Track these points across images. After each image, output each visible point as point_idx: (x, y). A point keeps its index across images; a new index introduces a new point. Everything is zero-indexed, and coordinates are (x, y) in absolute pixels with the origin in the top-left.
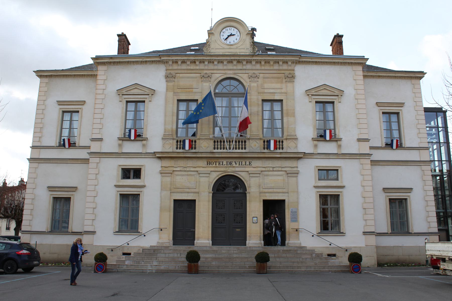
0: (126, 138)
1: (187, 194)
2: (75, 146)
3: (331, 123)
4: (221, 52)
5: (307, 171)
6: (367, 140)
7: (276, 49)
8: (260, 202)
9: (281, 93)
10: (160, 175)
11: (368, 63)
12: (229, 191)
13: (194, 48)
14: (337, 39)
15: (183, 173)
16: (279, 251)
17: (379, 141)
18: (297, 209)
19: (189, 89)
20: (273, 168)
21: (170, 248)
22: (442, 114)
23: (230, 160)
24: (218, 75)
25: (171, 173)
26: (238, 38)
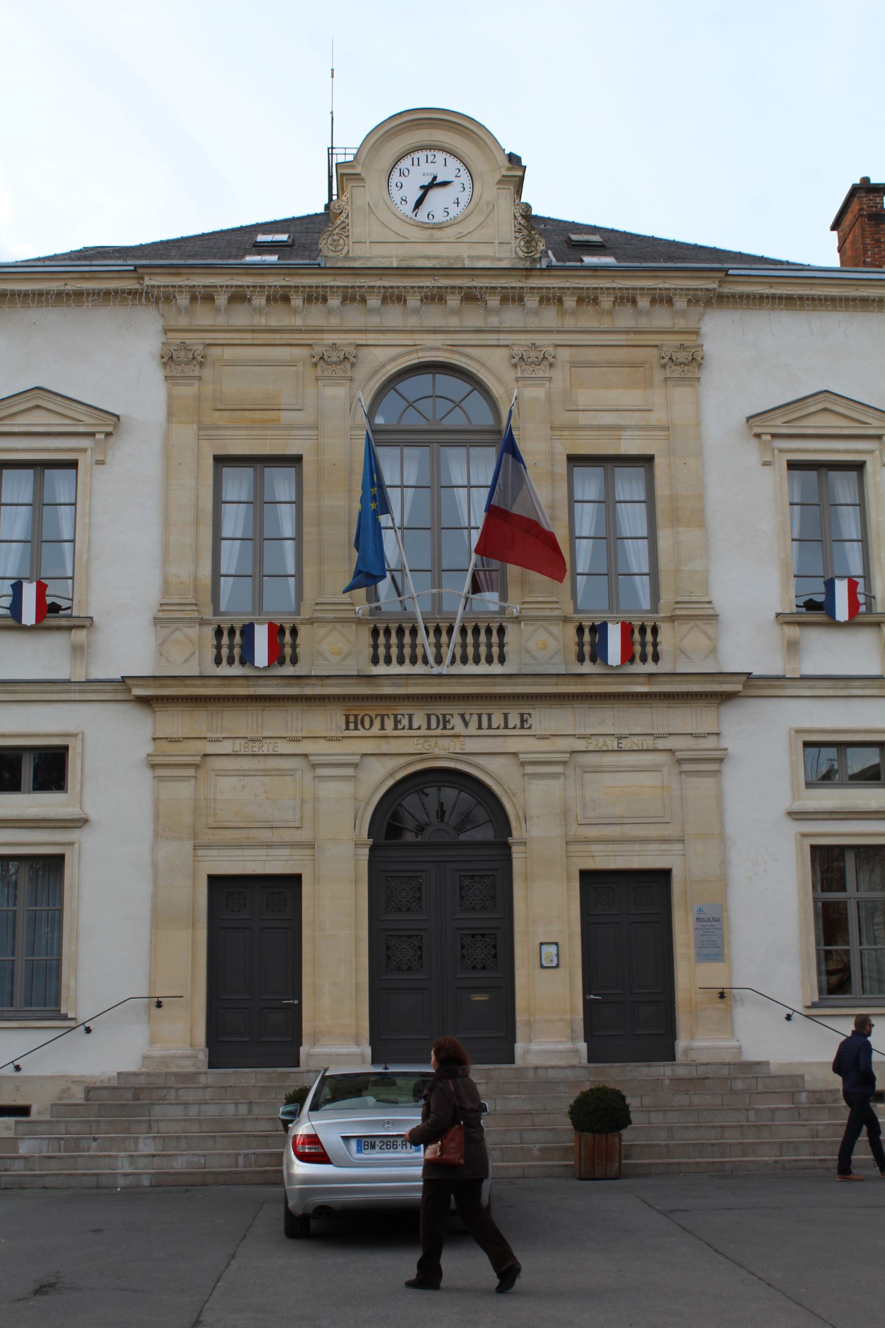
1: (263, 852)
3: (854, 552)
4: (392, 256)
5: (761, 750)
7: (610, 241)
8: (569, 879)
10: (148, 773)
14: (864, 199)
16: (658, 1082)
18: (722, 907)
19: (263, 411)
20: (620, 737)
21: (203, 1080)
23: (441, 709)
24: (381, 354)
25: (197, 766)
26: (464, 198)
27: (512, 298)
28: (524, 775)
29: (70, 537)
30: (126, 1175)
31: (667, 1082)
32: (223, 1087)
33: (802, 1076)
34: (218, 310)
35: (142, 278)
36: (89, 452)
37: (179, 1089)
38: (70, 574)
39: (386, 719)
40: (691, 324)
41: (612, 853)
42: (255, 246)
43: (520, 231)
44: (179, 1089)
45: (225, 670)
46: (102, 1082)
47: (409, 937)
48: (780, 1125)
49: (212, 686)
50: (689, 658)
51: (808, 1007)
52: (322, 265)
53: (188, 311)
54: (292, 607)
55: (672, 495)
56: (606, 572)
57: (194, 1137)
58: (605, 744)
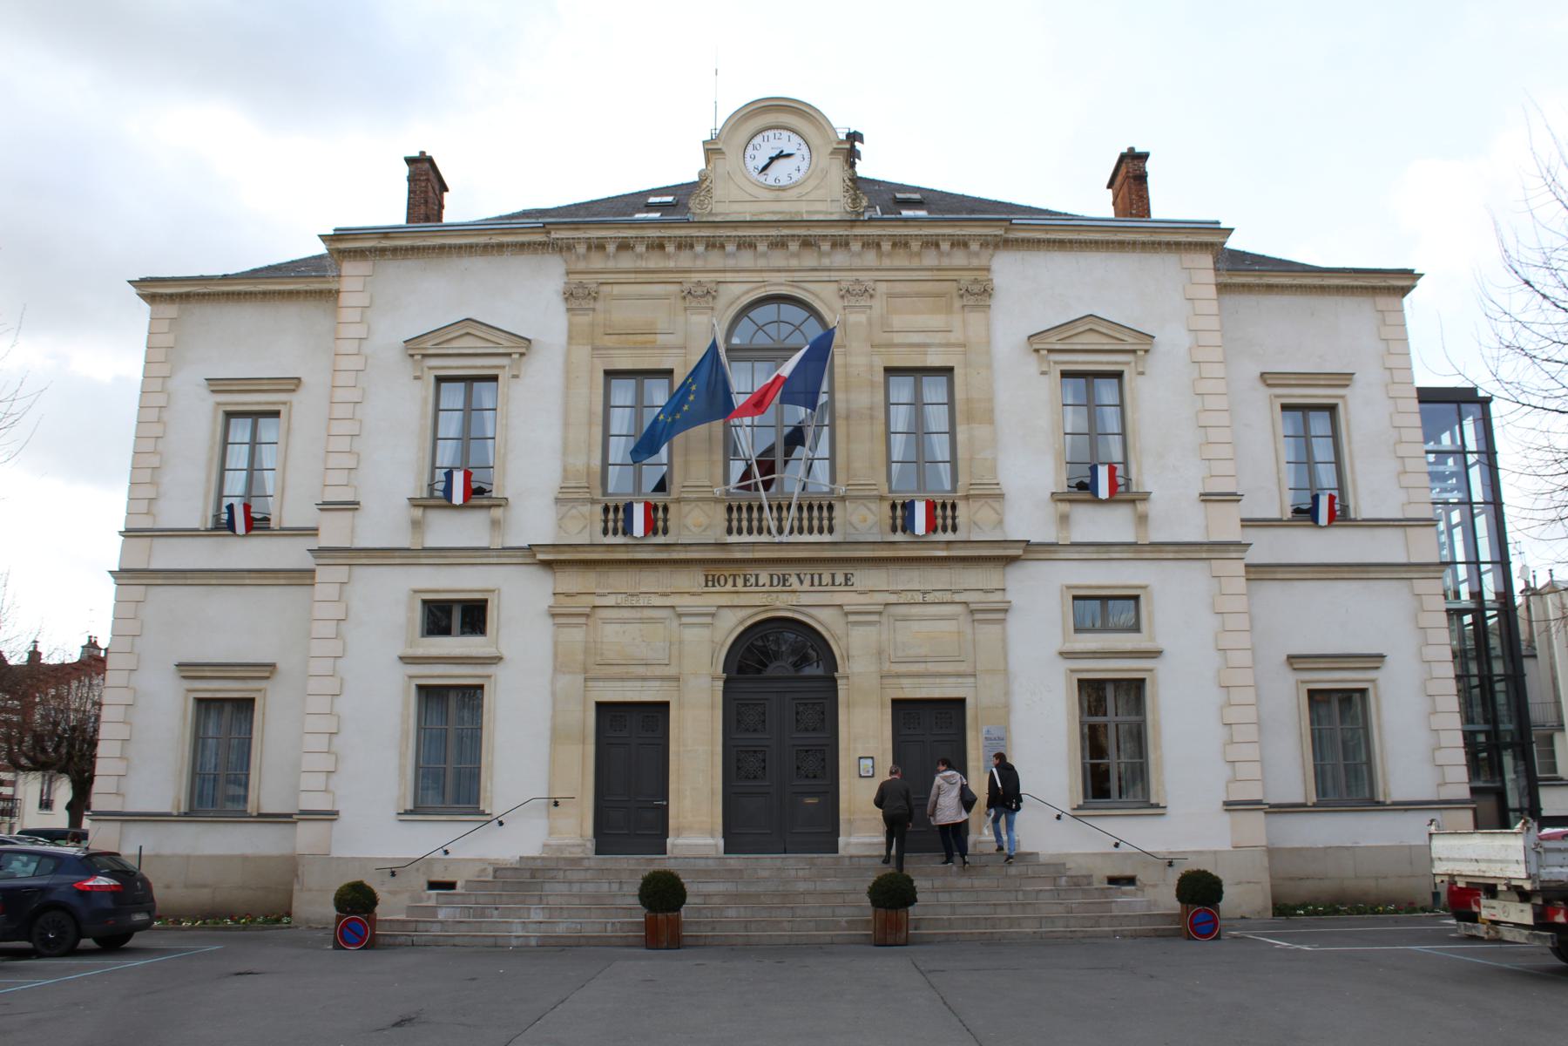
0: (436, 499)
1: (639, 684)
2: (268, 528)
4: (746, 212)
5: (1038, 603)
6: (1233, 498)
9: (947, 345)
10: (550, 621)
11: (1232, 243)
12: (779, 674)
14: (1129, 166)
15: (625, 613)
17: (1275, 504)
18: (1007, 729)
19: (643, 335)
20: (925, 593)
21: (586, 863)
22: (1476, 408)
23: (780, 570)
24: (736, 289)
25: (587, 616)
26: (804, 166)
27: (840, 243)
34: (608, 256)
40: (983, 262)
45: (610, 539)
53: (585, 257)
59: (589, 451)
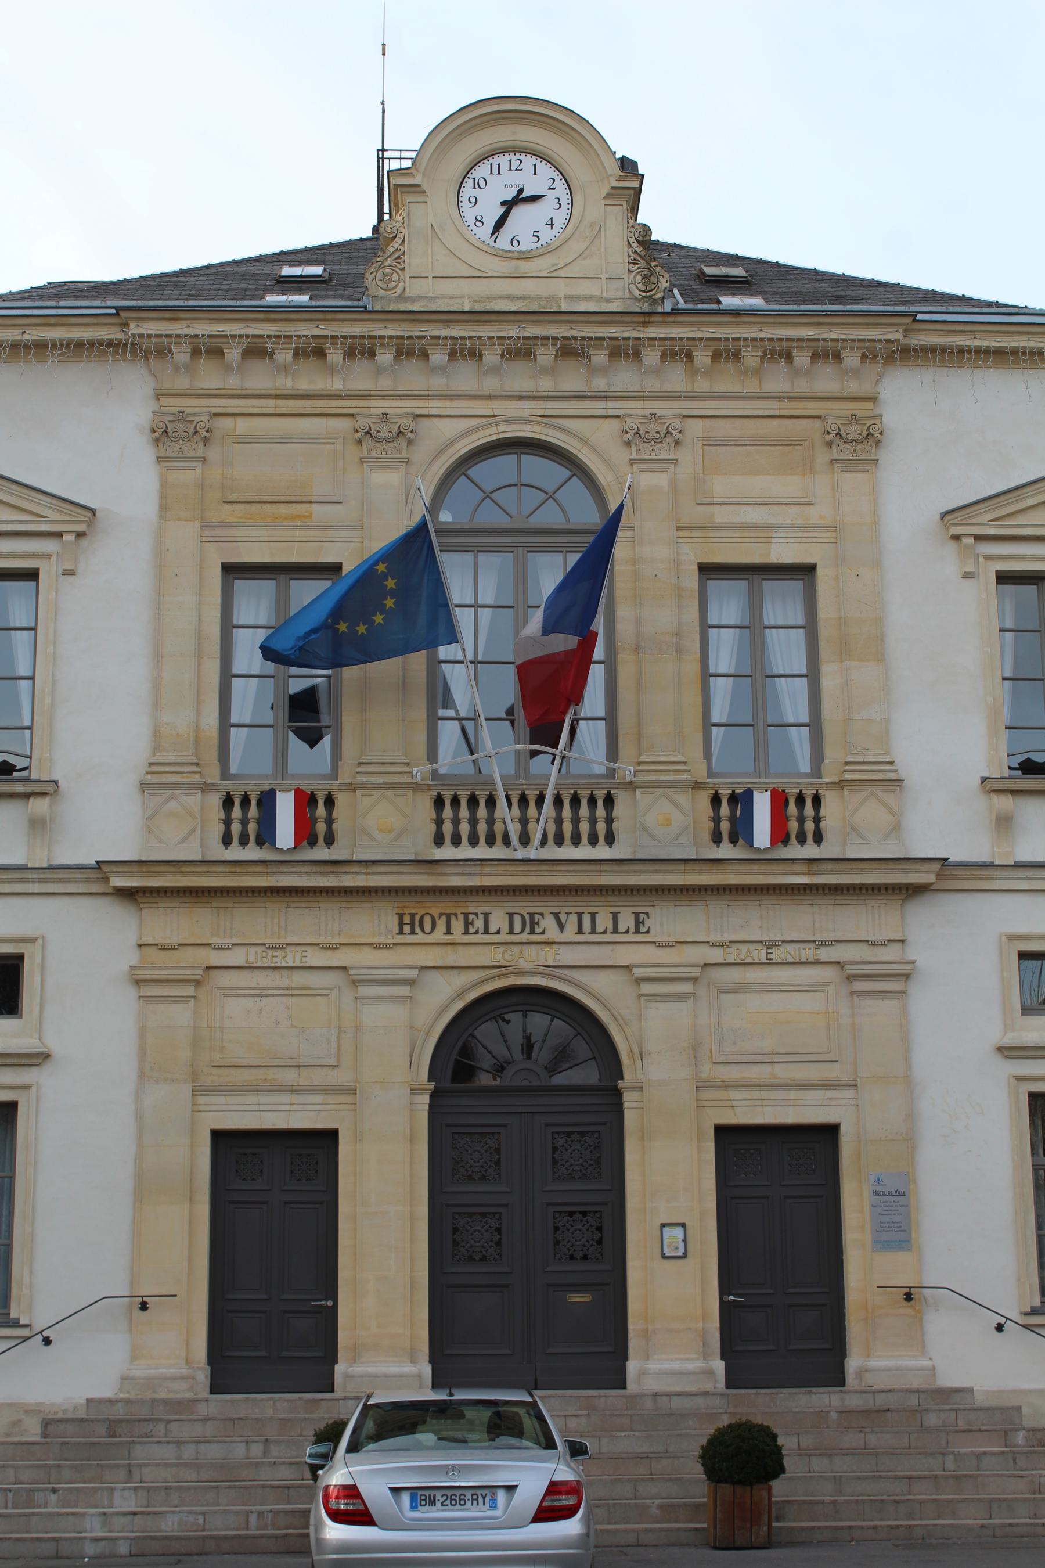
1: (285, 1099)
4: (462, 295)
8: (700, 1138)
9: (806, 527)
10: (132, 992)
13: (297, 271)
16: (822, 1415)
20: (770, 945)
21: (202, 1409)
23: (525, 907)
24: (449, 428)
25: (197, 983)
27: (625, 352)
28: (639, 996)
29: (29, 674)
30: (96, 1540)
31: (834, 1415)
32: (230, 1419)
33: (1019, 1409)
34: (228, 368)
35: (127, 325)
36: (54, 558)
37: (169, 1422)
38: (27, 723)
39: (453, 918)
40: (867, 387)
41: (759, 1103)
42: (278, 282)
43: (635, 262)
44: (169, 1422)
45: (235, 853)
46: (65, 1411)
47: (484, 1215)
48: (988, 1476)
49: (218, 874)
50: (863, 838)
51: (1026, 1314)
52: (369, 308)
54: (327, 769)
55: (840, 618)
56: (751, 722)
57: (189, 1488)
58: (749, 954)
59: (199, 702)
